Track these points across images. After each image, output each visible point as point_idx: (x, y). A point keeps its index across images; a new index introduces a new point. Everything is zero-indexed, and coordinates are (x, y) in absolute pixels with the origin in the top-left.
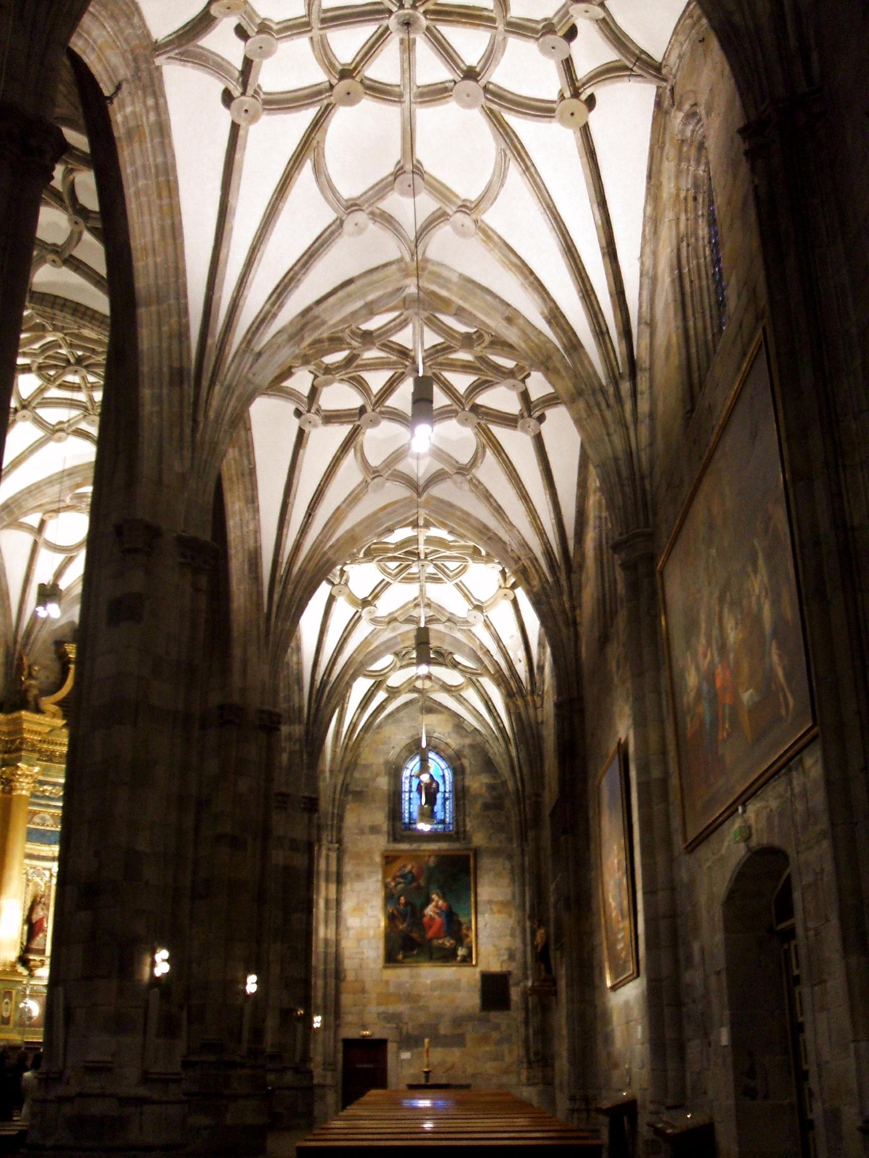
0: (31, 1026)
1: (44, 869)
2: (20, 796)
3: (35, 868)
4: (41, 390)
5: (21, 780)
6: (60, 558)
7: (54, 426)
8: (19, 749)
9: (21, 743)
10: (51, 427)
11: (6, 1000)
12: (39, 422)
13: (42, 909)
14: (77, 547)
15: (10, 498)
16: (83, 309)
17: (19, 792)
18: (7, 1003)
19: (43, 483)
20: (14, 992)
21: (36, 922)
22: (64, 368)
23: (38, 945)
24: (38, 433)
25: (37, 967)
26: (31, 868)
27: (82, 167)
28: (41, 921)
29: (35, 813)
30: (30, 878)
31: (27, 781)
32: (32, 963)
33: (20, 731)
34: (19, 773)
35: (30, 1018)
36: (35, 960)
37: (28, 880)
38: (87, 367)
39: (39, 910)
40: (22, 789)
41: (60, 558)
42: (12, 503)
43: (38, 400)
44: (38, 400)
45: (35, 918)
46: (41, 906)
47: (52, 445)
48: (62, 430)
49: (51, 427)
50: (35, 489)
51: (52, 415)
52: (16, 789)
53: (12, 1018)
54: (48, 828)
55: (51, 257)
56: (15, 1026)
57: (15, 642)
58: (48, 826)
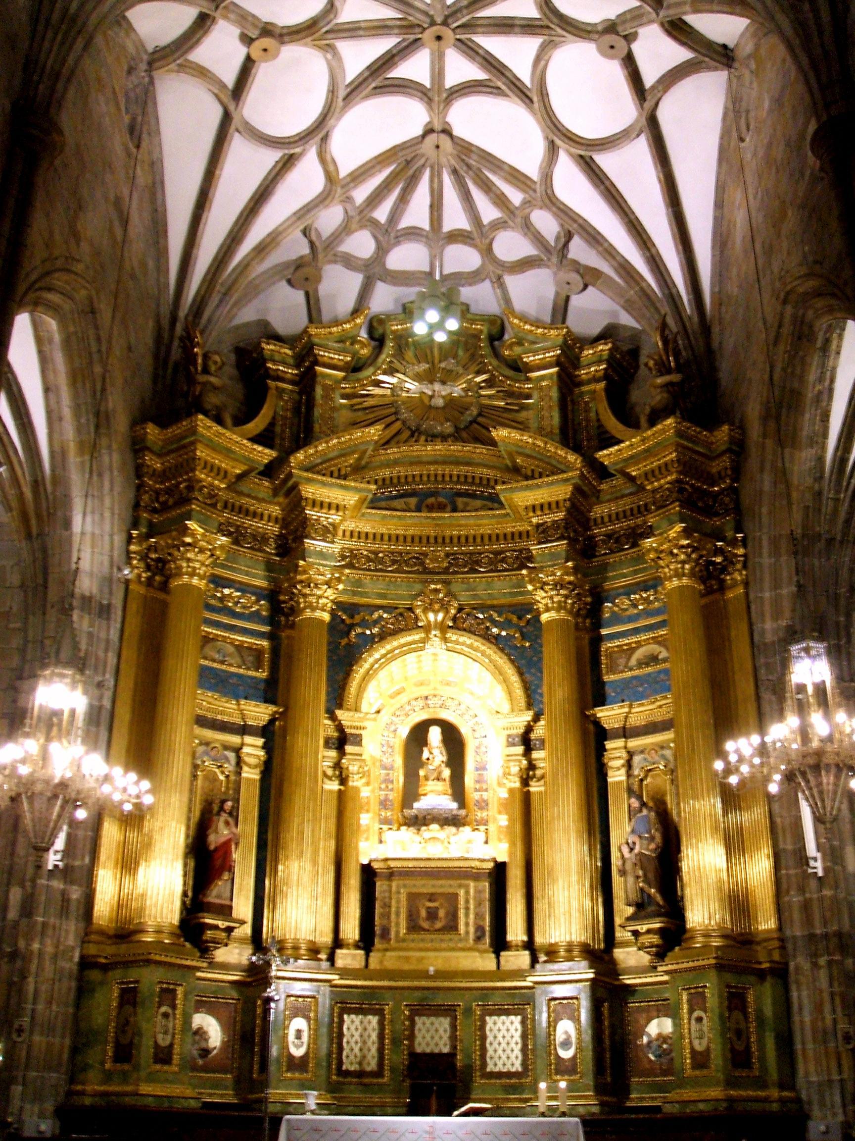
0: (205, 1069)
1: (226, 747)
2: (188, 587)
3: (207, 744)
5: (189, 555)
8: (187, 501)
9: (190, 488)
11: (164, 1009)
13: (227, 823)
14: (301, 139)
17: (186, 578)
18: (166, 1015)
20: (180, 991)
21: (216, 849)
23: (219, 896)
25: (217, 943)
26: (201, 744)
28: (225, 848)
29: (207, 640)
30: (199, 762)
31: (200, 557)
32: (209, 934)
33: (189, 464)
34: (188, 540)
35: (205, 1052)
36: (216, 927)
37: (195, 767)
39: (221, 825)
40: (192, 575)
41: (271, 157)
45: (214, 840)
46: (224, 816)
52: (180, 574)
53: (177, 1049)
54: (232, 669)
56: (182, 1067)
57: (174, 319)
58: (231, 665)
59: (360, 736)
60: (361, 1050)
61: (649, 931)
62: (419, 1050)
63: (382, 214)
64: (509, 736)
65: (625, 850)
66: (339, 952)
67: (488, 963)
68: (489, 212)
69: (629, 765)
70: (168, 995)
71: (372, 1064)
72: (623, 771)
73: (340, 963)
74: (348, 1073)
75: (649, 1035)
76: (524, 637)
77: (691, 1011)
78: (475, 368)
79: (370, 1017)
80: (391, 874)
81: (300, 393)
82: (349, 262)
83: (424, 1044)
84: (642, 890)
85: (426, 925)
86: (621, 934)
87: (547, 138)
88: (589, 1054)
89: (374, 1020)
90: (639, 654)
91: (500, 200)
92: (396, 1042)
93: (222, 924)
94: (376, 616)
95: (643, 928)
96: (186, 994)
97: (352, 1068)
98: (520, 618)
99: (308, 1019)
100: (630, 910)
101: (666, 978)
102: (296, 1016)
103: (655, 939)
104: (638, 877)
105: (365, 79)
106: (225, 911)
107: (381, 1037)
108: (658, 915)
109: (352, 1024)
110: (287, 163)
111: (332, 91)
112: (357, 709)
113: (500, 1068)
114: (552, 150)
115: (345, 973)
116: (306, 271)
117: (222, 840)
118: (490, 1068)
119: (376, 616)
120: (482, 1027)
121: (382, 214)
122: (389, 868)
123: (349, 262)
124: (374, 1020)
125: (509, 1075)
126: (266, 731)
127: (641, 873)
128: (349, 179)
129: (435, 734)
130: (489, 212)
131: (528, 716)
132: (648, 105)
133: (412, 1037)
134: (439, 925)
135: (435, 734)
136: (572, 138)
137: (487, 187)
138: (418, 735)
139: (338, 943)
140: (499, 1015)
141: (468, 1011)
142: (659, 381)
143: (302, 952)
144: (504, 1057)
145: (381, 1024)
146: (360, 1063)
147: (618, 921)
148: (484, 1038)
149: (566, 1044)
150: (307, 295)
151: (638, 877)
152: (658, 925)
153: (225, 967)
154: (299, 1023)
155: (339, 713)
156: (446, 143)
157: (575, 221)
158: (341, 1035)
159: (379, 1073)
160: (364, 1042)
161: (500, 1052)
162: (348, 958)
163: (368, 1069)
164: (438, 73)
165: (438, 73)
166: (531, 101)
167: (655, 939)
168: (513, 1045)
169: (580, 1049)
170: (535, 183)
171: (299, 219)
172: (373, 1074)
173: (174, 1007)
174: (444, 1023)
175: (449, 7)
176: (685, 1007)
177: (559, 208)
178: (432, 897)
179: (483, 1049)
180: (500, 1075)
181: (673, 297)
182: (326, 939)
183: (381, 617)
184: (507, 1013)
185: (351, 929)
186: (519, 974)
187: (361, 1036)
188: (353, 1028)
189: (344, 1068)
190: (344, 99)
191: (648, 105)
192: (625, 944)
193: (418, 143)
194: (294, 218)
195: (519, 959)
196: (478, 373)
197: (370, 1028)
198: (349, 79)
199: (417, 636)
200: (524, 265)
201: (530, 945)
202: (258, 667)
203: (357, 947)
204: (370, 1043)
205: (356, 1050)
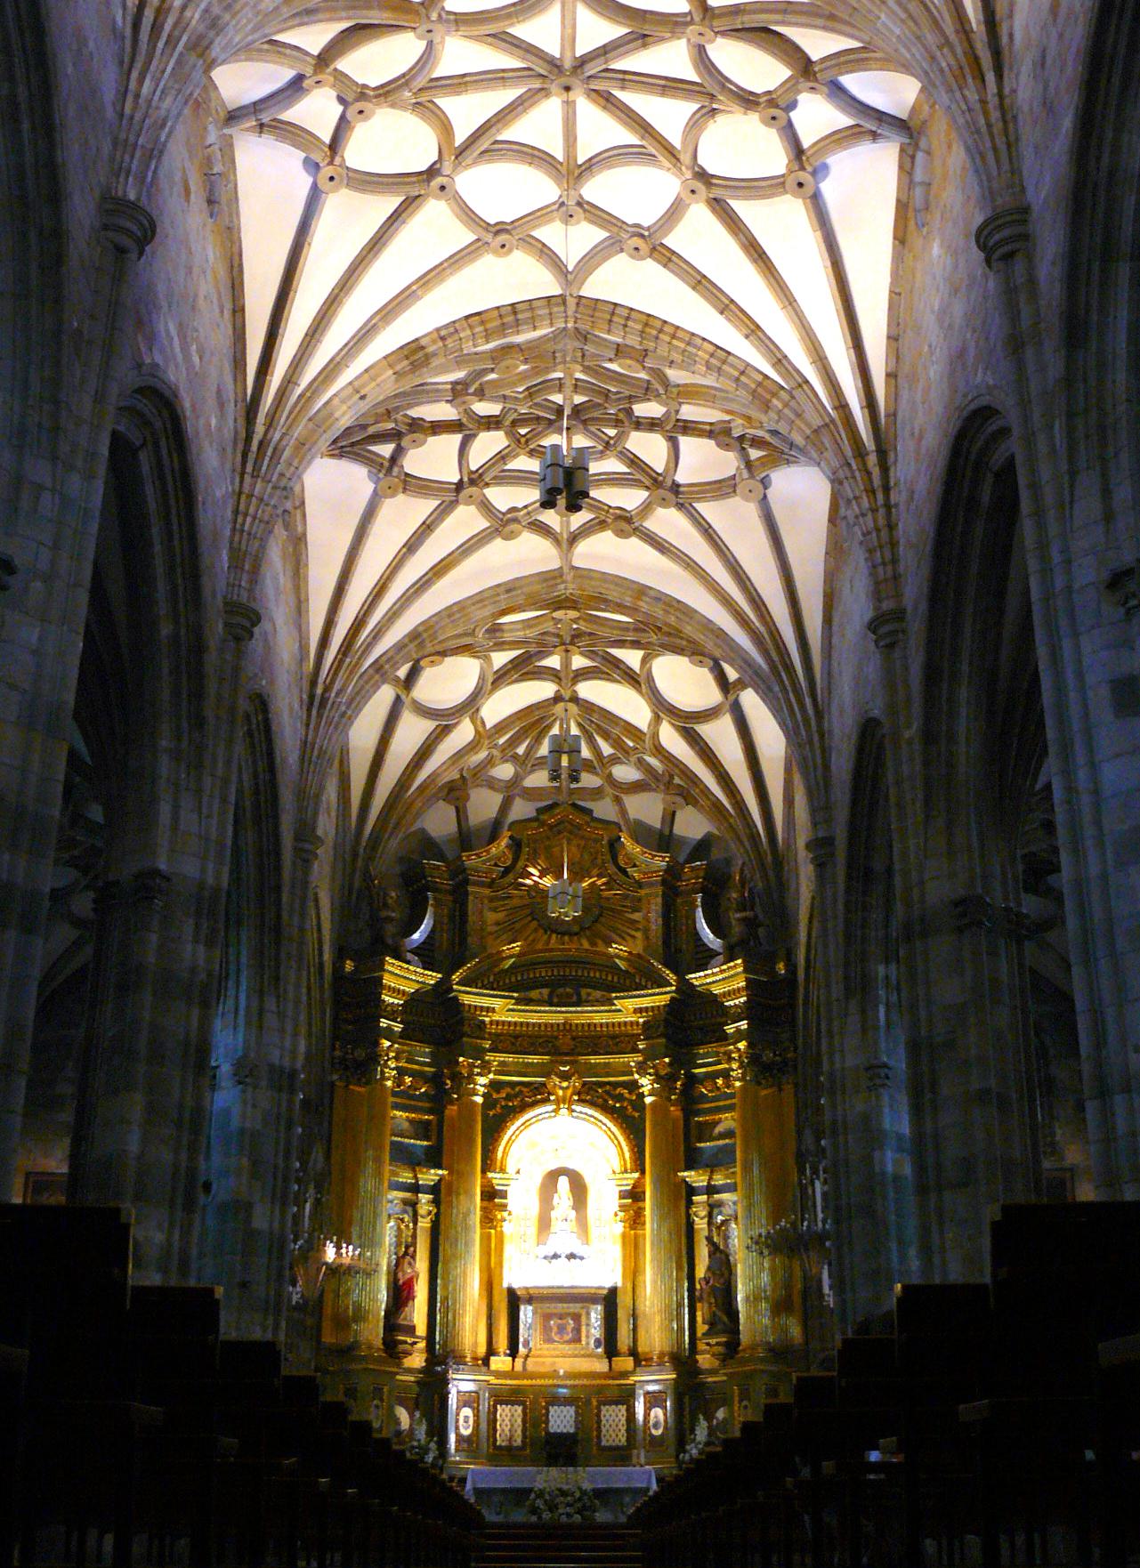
4: (502, 457)
6: (429, 725)
7: (504, 514)
10: (501, 516)
11: (375, 1402)
12: (486, 507)
13: (410, 1264)
15: (423, 623)
16: (658, 324)
18: (377, 1407)
19: (470, 602)
20: (385, 1389)
22: (550, 422)
24: (482, 523)
27: (736, 108)
36: (406, 1342)
38: (585, 422)
39: (406, 1266)
41: (429, 725)
42: (425, 631)
43: (494, 473)
44: (494, 473)
47: (498, 542)
48: (516, 520)
49: (501, 516)
50: (459, 611)
51: (503, 497)
55: (636, 241)
57: (355, 855)
59: (506, 1191)
60: (510, 1430)
61: (717, 1344)
62: (552, 1431)
63: (521, 750)
64: (620, 1192)
65: (703, 1283)
66: (492, 1358)
67: (601, 1366)
68: (607, 749)
69: (710, 1216)
70: (378, 1392)
71: (518, 1441)
72: (706, 1220)
73: (493, 1367)
74: (500, 1448)
75: (717, 1419)
76: (634, 1109)
77: (741, 1401)
78: (595, 872)
79: (516, 1407)
80: (530, 1300)
81: (455, 901)
82: (492, 784)
83: (555, 1427)
84: (714, 1312)
85: (556, 1339)
86: (701, 1346)
87: (653, 711)
88: (672, 1433)
89: (519, 1409)
90: (719, 1129)
91: (617, 743)
92: (536, 1425)
93: (409, 1340)
94: (517, 1089)
95: (713, 1341)
96: (390, 1392)
97: (503, 1444)
98: (630, 1093)
99: (473, 1409)
100: (706, 1327)
101: (725, 1378)
102: (465, 1406)
103: (720, 1349)
104: (711, 1303)
105: (509, 671)
106: (411, 1330)
107: (524, 1422)
108: (724, 1332)
109: (503, 1412)
110: (444, 731)
111: (482, 678)
112: (503, 1170)
113: (610, 1443)
114: (657, 720)
115: (498, 1374)
116: (456, 794)
117: (407, 1276)
118: (604, 1443)
119: (517, 1089)
120: (598, 1415)
121: (521, 750)
122: (528, 1294)
123: (492, 784)
124: (519, 1409)
125: (618, 1448)
126: (435, 1190)
127: (713, 1300)
128: (493, 731)
129: (563, 1182)
130: (607, 749)
131: (636, 1175)
132: (732, 698)
133: (547, 1422)
134: (567, 1338)
135: (563, 1182)
136: (673, 712)
137: (607, 736)
138: (553, 1176)
139: (491, 1351)
140: (610, 1405)
141: (588, 1402)
142: (738, 915)
143: (468, 1359)
144: (614, 1435)
145: (524, 1411)
146: (510, 1440)
147: (699, 1334)
148: (599, 1422)
149: (656, 1426)
150: (457, 808)
151: (711, 1303)
152: (724, 1339)
153: (410, 1371)
154: (467, 1412)
155: (490, 1175)
156: (573, 708)
157: (677, 766)
158: (495, 1420)
159: (522, 1448)
160: (512, 1425)
161: (611, 1432)
162: (500, 1362)
163: (515, 1444)
164: (566, 663)
165: (566, 663)
166: (638, 683)
167: (720, 1349)
168: (620, 1426)
169: (666, 1428)
170: (645, 734)
171: (453, 764)
172: (518, 1448)
173: (382, 1400)
174: (569, 1412)
175: (581, 166)
176: (737, 1399)
177: (664, 756)
178: (561, 1317)
179: (599, 1429)
180: (611, 1448)
181: (754, 837)
182: (482, 1350)
183: (521, 1092)
184: (617, 1403)
185: (502, 1342)
186: (625, 1375)
187: (510, 1421)
188: (504, 1414)
189: (498, 1443)
190: (493, 683)
191: (732, 698)
192: (703, 1352)
193: (549, 705)
194: (450, 762)
195: (628, 1363)
196: (600, 876)
197: (516, 1414)
198: (496, 668)
199: (550, 1107)
200: (636, 787)
201: (633, 1352)
202: (427, 1138)
203: (506, 1355)
204: (516, 1426)
205: (507, 1430)
